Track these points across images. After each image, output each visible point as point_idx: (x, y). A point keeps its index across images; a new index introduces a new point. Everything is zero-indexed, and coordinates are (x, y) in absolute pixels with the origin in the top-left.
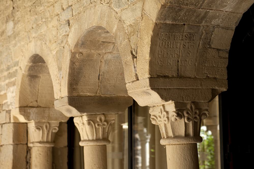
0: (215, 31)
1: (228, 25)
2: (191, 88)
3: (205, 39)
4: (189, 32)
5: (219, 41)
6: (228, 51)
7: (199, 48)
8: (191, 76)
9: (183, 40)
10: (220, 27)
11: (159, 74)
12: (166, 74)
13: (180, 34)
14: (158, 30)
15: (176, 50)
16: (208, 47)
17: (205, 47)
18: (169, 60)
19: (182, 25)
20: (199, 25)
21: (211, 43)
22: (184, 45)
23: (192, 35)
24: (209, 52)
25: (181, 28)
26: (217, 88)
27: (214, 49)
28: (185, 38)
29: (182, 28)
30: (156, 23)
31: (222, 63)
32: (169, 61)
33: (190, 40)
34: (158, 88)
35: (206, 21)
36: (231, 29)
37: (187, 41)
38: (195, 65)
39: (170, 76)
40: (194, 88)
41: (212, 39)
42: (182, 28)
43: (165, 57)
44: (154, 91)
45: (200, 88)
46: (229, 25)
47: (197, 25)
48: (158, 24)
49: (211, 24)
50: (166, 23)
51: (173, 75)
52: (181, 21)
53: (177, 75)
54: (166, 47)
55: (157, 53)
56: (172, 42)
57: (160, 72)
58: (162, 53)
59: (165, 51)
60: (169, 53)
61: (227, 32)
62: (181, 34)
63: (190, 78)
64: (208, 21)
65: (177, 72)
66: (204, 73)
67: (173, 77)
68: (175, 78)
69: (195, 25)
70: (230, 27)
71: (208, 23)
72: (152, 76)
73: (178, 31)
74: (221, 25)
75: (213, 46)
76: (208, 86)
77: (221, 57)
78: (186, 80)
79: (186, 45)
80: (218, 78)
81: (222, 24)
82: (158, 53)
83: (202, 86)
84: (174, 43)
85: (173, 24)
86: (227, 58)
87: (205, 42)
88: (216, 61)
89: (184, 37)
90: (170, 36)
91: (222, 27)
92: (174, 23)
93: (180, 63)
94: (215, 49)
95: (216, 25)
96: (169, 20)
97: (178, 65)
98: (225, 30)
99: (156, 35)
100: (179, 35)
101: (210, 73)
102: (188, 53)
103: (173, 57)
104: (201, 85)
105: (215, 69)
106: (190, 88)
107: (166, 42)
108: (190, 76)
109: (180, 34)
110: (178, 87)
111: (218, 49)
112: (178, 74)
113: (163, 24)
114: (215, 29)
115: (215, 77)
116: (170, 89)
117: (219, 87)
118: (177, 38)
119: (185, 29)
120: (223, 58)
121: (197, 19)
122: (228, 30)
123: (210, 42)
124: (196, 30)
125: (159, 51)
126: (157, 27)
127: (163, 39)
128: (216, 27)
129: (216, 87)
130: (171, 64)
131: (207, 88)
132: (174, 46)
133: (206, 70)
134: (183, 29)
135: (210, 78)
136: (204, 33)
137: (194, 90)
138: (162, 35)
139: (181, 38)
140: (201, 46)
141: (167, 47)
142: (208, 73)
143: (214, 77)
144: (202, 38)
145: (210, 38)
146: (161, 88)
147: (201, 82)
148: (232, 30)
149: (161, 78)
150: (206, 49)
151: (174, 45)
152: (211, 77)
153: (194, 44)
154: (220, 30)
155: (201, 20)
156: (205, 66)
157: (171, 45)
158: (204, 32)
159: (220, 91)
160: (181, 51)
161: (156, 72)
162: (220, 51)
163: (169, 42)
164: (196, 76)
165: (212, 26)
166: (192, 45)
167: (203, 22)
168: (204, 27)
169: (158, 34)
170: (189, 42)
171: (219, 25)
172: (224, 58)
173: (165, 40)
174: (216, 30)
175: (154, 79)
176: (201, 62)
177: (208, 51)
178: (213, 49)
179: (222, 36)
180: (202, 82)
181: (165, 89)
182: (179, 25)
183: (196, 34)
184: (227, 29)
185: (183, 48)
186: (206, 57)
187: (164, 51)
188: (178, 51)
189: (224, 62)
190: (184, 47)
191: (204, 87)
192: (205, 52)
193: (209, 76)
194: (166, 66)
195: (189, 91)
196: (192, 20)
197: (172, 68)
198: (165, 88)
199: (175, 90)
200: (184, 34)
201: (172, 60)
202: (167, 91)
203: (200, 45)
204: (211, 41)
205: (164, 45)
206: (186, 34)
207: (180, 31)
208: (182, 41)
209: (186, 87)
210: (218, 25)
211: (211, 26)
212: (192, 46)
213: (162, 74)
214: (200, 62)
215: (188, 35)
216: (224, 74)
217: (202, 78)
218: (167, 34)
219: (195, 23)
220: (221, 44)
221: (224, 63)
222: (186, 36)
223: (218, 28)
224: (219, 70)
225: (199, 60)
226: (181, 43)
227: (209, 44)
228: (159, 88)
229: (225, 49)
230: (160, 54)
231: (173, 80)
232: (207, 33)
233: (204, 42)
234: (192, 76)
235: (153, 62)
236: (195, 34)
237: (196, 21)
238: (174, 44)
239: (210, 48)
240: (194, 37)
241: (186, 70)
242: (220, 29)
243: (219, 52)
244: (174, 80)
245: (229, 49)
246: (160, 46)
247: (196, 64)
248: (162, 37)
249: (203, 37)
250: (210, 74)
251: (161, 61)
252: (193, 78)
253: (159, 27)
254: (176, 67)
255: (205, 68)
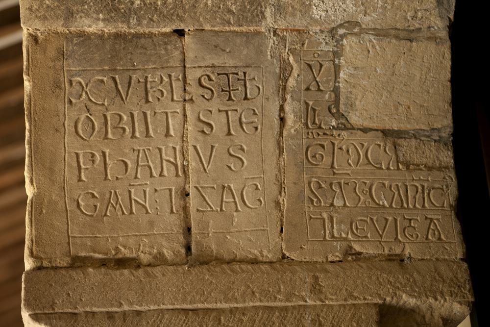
0: (348, 48)
1: (406, 18)
2: (258, 304)
3: (308, 89)
4: (213, 66)
5: (385, 93)
6: (444, 135)
7: (285, 133)
8: (261, 252)
9: (191, 100)
10: (363, 31)
11: (83, 254)
12: (123, 249)
13: (170, 76)
14: (51, 64)
15: (167, 147)
16: (334, 123)
17: (320, 127)
18: (133, 191)
19: (165, 35)
20: (252, 28)
21: (346, 105)
22: (201, 125)
23: (231, 76)
24: (344, 147)
25: (166, 49)
26: (408, 300)
27: (365, 130)
28: (201, 91)
29: (169, 47)
30: (30, 34)
31: (426, 192)
32: (133, 196)
33: (230, 99)
34: (75, 314)
35: (280, 9)
36: (429, 39)
37: (216, 104)
38: (278, 204)
39: (145, 258)
40: (278, 304)
41: (342, 90)
42: (169, 47)
43: (109, 177)
44: (46, 324)
45: (310, 302)
46: (409, 18)
47: (244, 29)
48: (45, 40)
49: (312, 18)
50: (82, 34)
51: (161, 255)
52: (155, 18)
53: (183, 251)
54: (110, 136)
55: (70, 166)
56: (136, 114)
57: (89, 243)
58: (93, 162)
59: (107, 154)
60: (129, 162)
61: (410, 50)
62: (173, 78)
63: (255, 262)
64: (292, 7)
65: (181, 238)
66: (327, 238)
67: (160, 260)
68: (173, 264)
69: (235, 32)
70: (417, 26)
71: (293, 15)
72: (46, 264)
73: (155, 63)
74: (365, 21)
75: (355, 119)
76: (355, 294)
77: (412, 167)
78: (232, 271)
79: (213, 124)
80: (410, 258)
81: (368, 18)
82: (75, 164)
83: (320, 292)
84: (149, 117)
85: (118, 36)
86: (446, 168)
87: (311, 103)
88: (387, 183)
89: (194, 90)
90: (119, 87)
91: (374, 29)
92: (123, 28)
93: (193, 202)
94: (371, 130)
95: (339, 22)
96: (87, 15)
97: (185, 209)
98: (394, 41)
99: (48, 88)
100: (166, 79)
101: (366, 237)
102: (230, 155)
103: (154, 174)
104: (316, 289)
105: (390, 219)
106: (254, 306)
107: (105, 116)
108: (256, 252)
109: (170, 76)
110: (184, 301)
111: (386, 133)
112: (188, 249)
113: (69, 37)
114: (345, 41)
115: (396, 255)
116: (139, 313)
117: (419, 293)
118: (158, 95)
119: (190, 55)
120: (422, 167)
121: (229, 3)
122: (411, 41)
123: (337, 102)
124: (245, 52)
125: (77, 154)
126: (44, 51)
127: (88, 103)
128: (341, 31)
129: (404, 296)
130: (147, 206)
131: (350, 302)
132: (151, 131)
133: (340, 222)
134: (177, 53)
135: (369, 259)
136: (295, 66)
137: (277, 314)
138: (78, 88)
139: (181, 92)
140: (295, 122)
141: (113, 134)
142: (350, 236)
143: (389, 255)
144: (289, 88)
145: (331, 84)
146: (88, 309)
147: (316, 278)
148: (433, 38)
149: (91, 270)
150: (324, 134)
151: (150, 126)
152: (371, 252)
153: (255, 114)
154: (373, 46)
155: (251, 3)
156: (332, 205)
157: (136, 124)
158: (291, 59)
159: (436, 314)
160: (191, 150)
161: (67, 245)
162: (401, 141)
163: (121, 117)
164: (287, 254)
165: (322, 32)
166: (243, 120)
167: (268, 13)
168: (283, 39)
169: (57, 85)
170: (226, 109)
171: (357, 24)
172: (430, 168)
173: (99, 108)
174: (351, 47)
175: (52, 273)
176: (306, 189)
177: (336, 143)
178: (359, 132)
179: (393, 74)
180: (321, 276)
181: (110, 316)
182: (151, 35)
183: (250, 69)
184: (409, 36)
185: (200, 137)
186: (332, 167)
187: (104, 154)
188: (178, 148)
189: (437, 186)
190: (203, 132)
191: (332, 299)
192: (323, 146)
193: (357, 247)
194: (120, 213)
195: (245, 319)
196: (206, 4)
197: (151, 224)
198: (110, 309)
199: (166, 316)
200: (189, 77)
201: (148, 190)
202: (119, 322)
203: (290, 118)
204: (342, 100)
205: (97, 129)
206: (198, 73)
207: (165, 65)
208: (188, 107)
209: (227, 300)
210: (351, 24)
211: (317, 29)
212: (247, 123)
213: (99, 253)
214: (302, 191)
215: (210, 79)
216: (443, 237)
217: (320, 260)
218: (105, 79)
219: (229, 23)
220: (397, 109)
221: (432, 192)
222: (201, 85)
223: (356, 34)
224: (410, 220)
225: (295, 183)
226: (185, 115)
227: (334, 111)
228: (80, 310)
229: (423, 127)
230: (83, 166)
231: (159, 275)
232: (310, 66)
233: (307, 104)
234: (265, 253)
235: (49, 202)
236: (248, 70)
237: (230, 11)
238: (149, 120)
239: (347, 127)
240: (248, 85)
241: (232, 230)
242: (370, 41)
243: (395, 146)
244: (163, 275)
245: (444, 127)
246: (77, 132)
247: (284, 200)
248: (81, 96)
249: (291, 82)
250: (359, 239)
251: (93, 196)
252: (271, 263)
253: (52, 52)
254: (174, 222)
255: (335, 215)
